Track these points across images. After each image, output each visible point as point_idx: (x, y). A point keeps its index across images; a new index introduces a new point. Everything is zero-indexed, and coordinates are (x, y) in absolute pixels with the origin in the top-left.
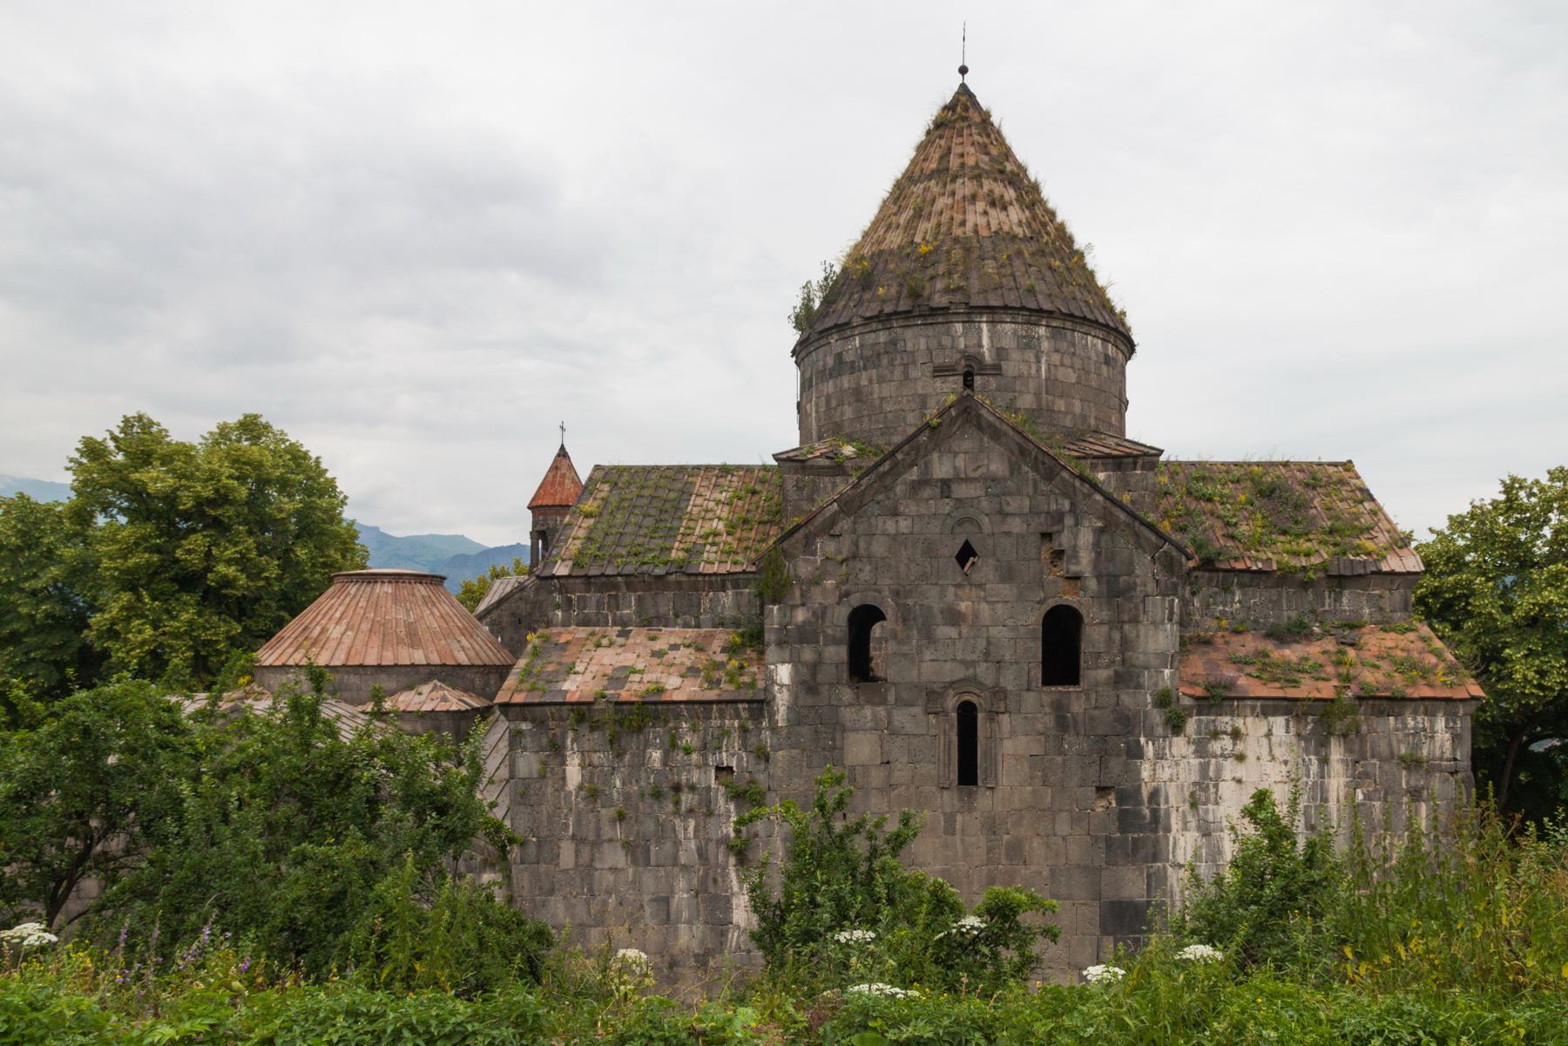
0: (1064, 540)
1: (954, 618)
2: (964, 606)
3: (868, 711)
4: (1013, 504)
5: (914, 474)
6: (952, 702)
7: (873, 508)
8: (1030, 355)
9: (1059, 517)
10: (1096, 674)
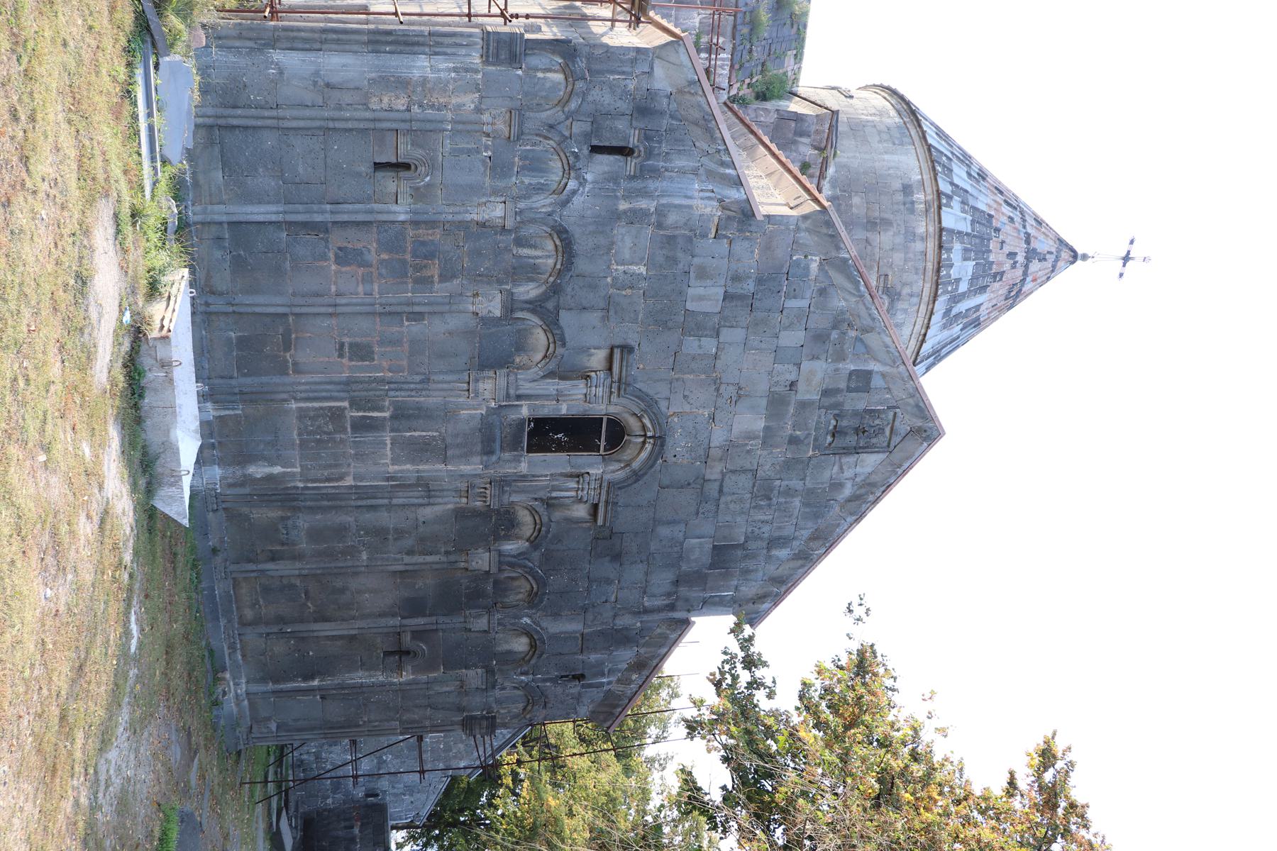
8: (874, 111)
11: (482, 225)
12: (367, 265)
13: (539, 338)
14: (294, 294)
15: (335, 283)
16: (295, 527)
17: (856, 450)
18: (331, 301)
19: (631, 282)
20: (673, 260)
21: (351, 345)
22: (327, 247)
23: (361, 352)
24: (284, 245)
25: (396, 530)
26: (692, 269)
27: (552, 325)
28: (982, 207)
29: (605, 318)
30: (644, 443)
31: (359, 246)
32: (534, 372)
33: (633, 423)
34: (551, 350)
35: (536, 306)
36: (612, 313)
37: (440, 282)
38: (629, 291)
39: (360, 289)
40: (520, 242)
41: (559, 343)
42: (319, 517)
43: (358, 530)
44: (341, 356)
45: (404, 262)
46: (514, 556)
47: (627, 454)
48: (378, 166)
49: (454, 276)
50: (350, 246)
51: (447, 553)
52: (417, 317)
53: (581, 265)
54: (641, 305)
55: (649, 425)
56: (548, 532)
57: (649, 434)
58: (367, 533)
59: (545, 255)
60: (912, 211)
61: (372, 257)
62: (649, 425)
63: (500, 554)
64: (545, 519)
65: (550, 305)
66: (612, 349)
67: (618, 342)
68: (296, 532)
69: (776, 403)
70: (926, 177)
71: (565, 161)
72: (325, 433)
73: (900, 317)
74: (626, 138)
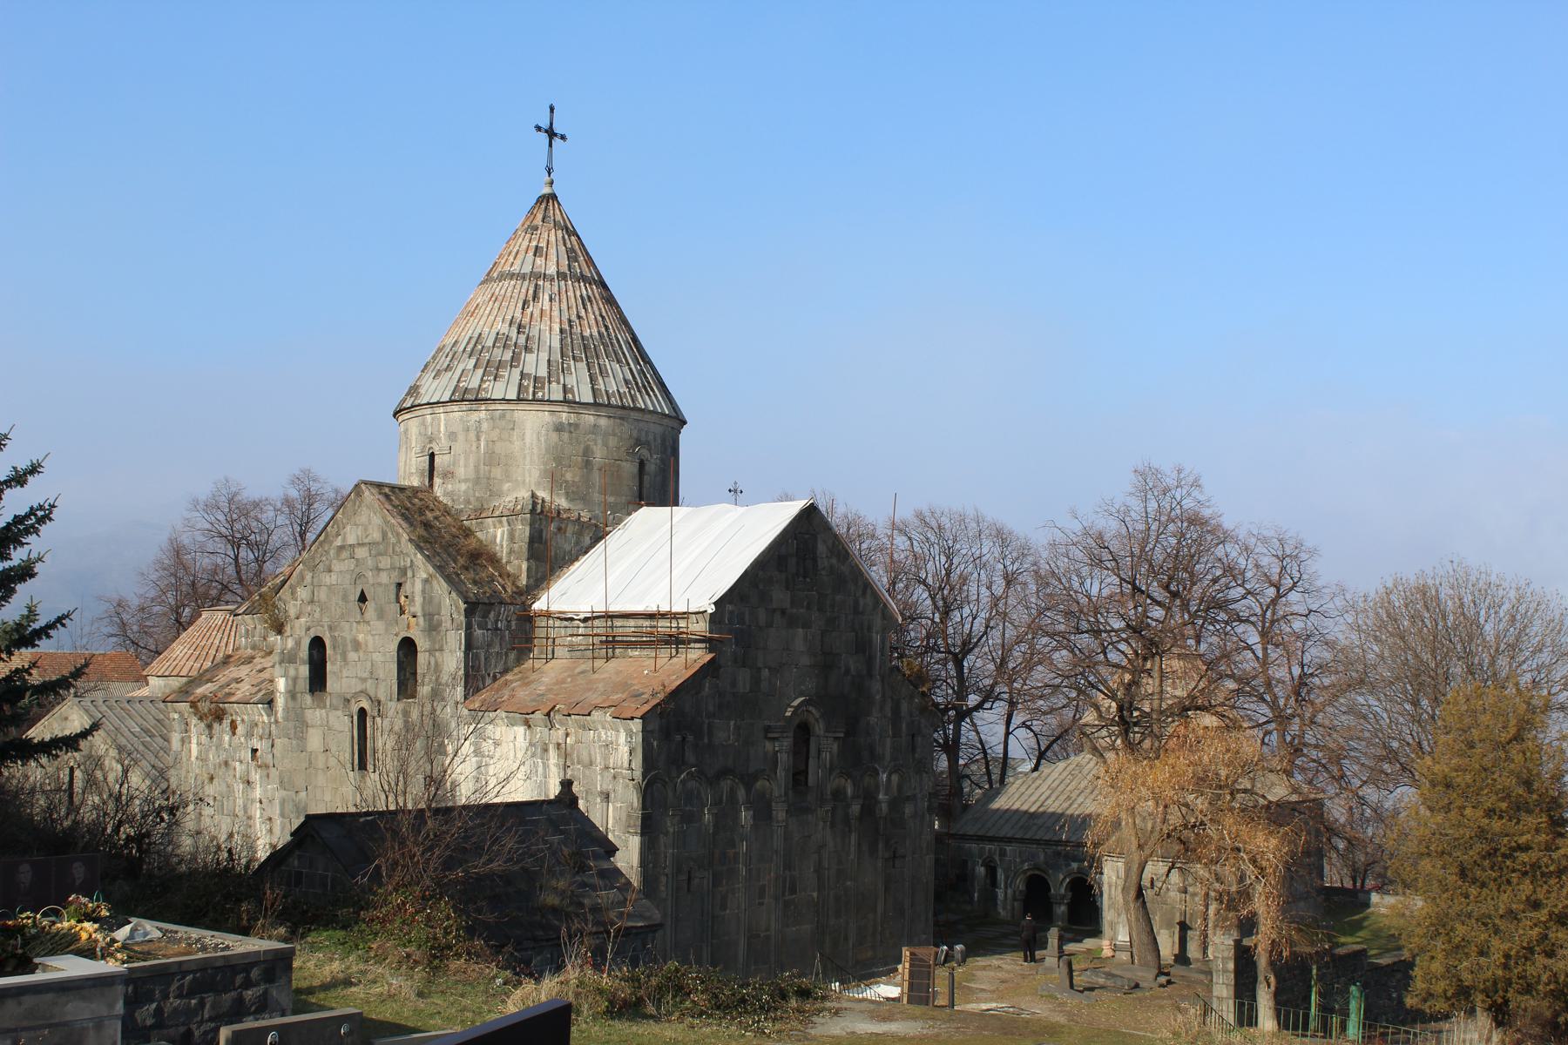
0: (407, 588)
1: (357, 646)
2: (361, 637)
3: (318, 712)
4: (385, 562)
5: (339, 542)
6: (355, 709)
7: (321, 567)
8: (472, 435)
9: (403, 571)
10: (424, 690)
17: (815, 560)
19: (737, 728)
27: (755, 777)
28: (556, 344)
47: (812, 720)
59: (726, 785)
60: (576, 426)
63: (853, 797)
69: (792, 622)
70: (547, 408)
73: (651, 437)
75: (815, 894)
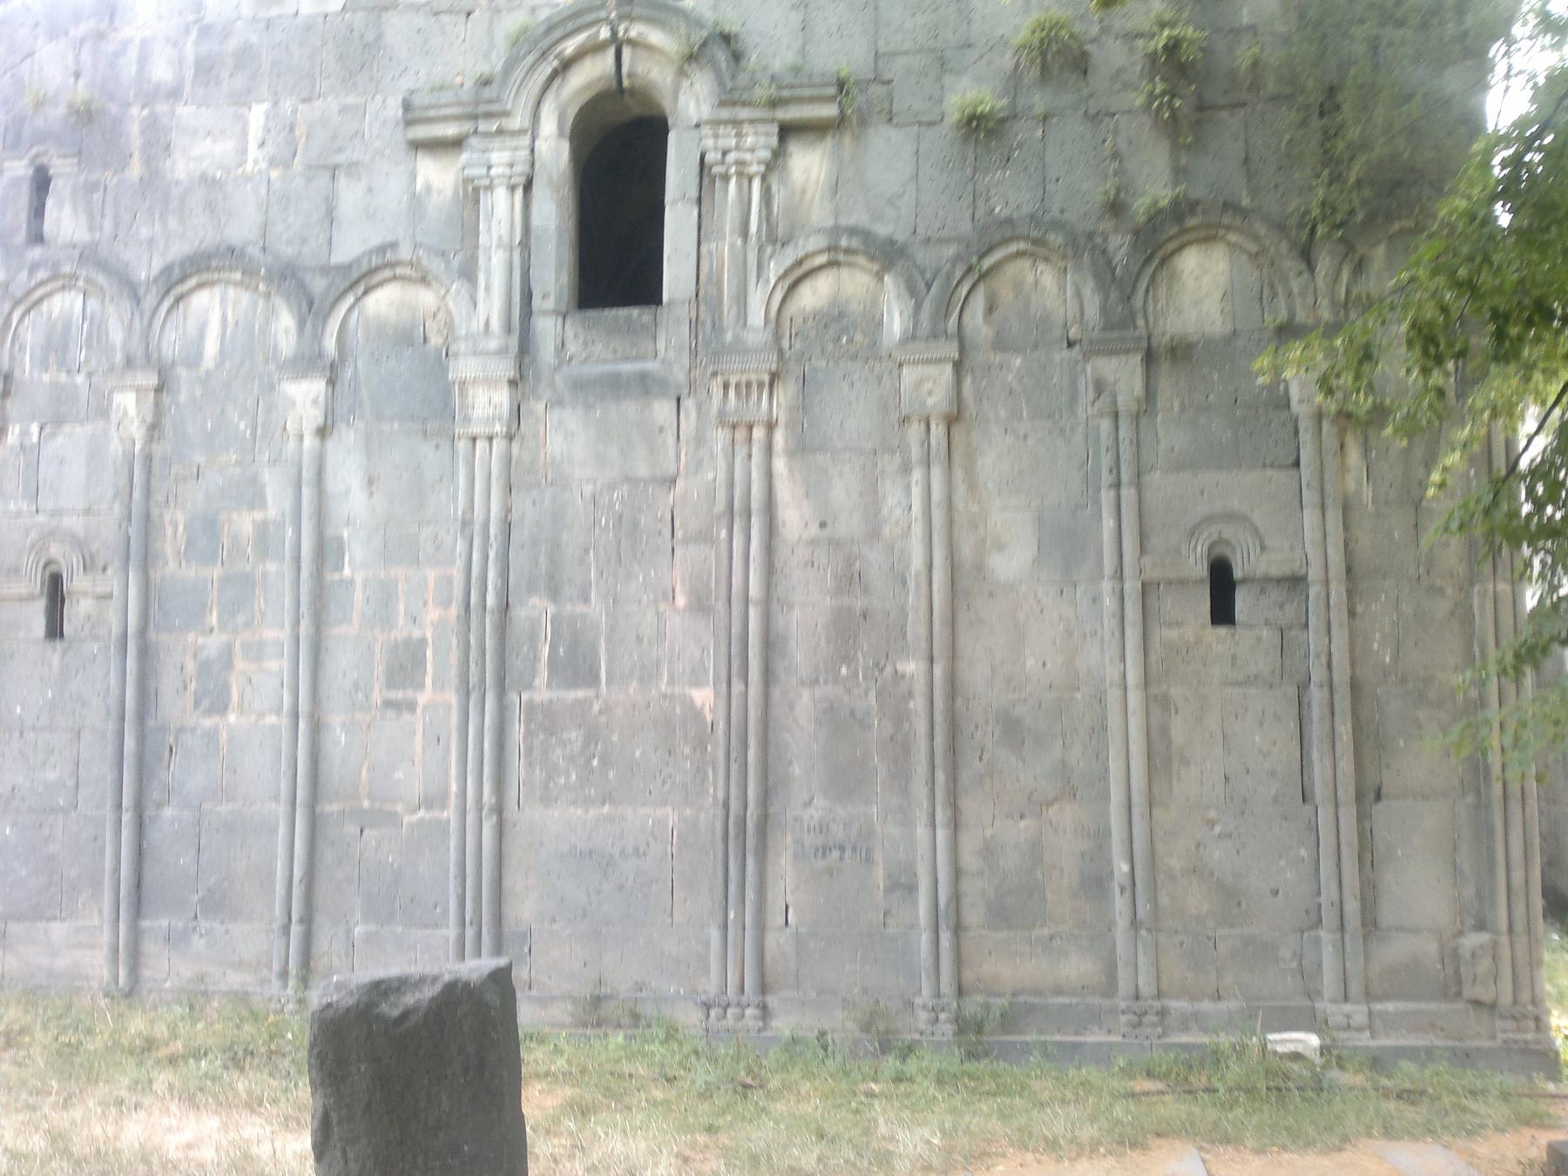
11: (154, 429)
12: (228, 650)
13: (383, 301)
14: (276, 798)
15: (261, 715)
16: (823, 828)
18: (285, 722)
20: (245, 56)
21: (391, 683)
22: (193, 730)
23: (406, 665)
24: (187, 814)
25: (839, 591)
26: (263, 14)
29: (353, 168)
30: (632, 43)
31: (191, 666)
32: (456, 302)
33: (591, 73)
34: (407, 271)
35: (312, 311)
36: (340, 158)
37: (263, 505)
38: (300, 131)
39: (273, 665)
40: (194, 359)
41: (389, 256)
42: (796, 770)
43: (837, 679)
44: (411, 706)
45: (226, 580)
46: (918, 306)
48: (55, 630)
49: (254, 481)
50: (192, 687)
51: (906, 469)
52: (326, 551)
53: (242, 229)
54: (328, 105)
55: (581, 38)
56: (852, 231)
57: (605, 33)
58: (847, 659)
61: (212, 644)
62: (581, 38)
63: (910, 337)
64: (816, 242)
65: (318, 285)
66: (418, 146)
67: (399, 136)
68: (834, 828)
71: (48, 288)
72: (586, 745)
74: (15, 183)
75: (704, 697)
